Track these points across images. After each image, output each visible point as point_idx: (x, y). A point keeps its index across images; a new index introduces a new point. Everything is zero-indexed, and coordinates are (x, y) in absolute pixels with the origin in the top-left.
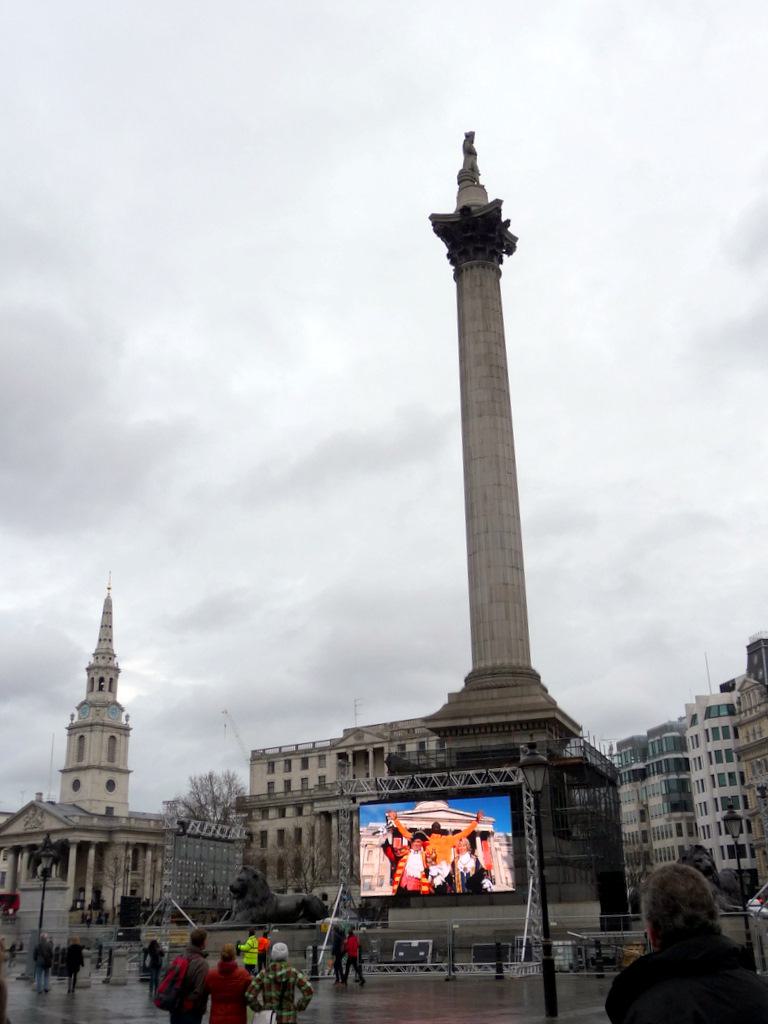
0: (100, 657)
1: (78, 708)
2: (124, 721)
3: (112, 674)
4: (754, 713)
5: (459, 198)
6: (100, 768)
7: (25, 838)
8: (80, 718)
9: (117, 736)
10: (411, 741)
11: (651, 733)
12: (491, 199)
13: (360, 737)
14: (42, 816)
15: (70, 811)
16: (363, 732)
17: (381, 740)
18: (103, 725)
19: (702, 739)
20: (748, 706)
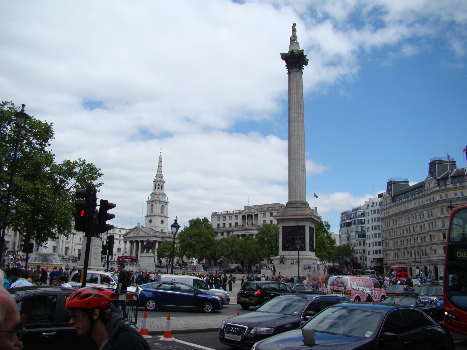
0: (158, 177)
1: (150, 195)
2: (166, 200)
3: (162, 183)
4: (387, 206)
5: (290, 46)
6: (159, 216)
7: (134, 238)
8: (151, 198)
9: (164, 205)
10: (267, 212)
11: (354, 210)
12: (301, 49)
13: (250, 210)
14: (140, 231)
15: (149, 230)
16: (251, 208)
17: (257, 211)
18: (160, 201)
19: (370, 214)
20: (386, 204)
